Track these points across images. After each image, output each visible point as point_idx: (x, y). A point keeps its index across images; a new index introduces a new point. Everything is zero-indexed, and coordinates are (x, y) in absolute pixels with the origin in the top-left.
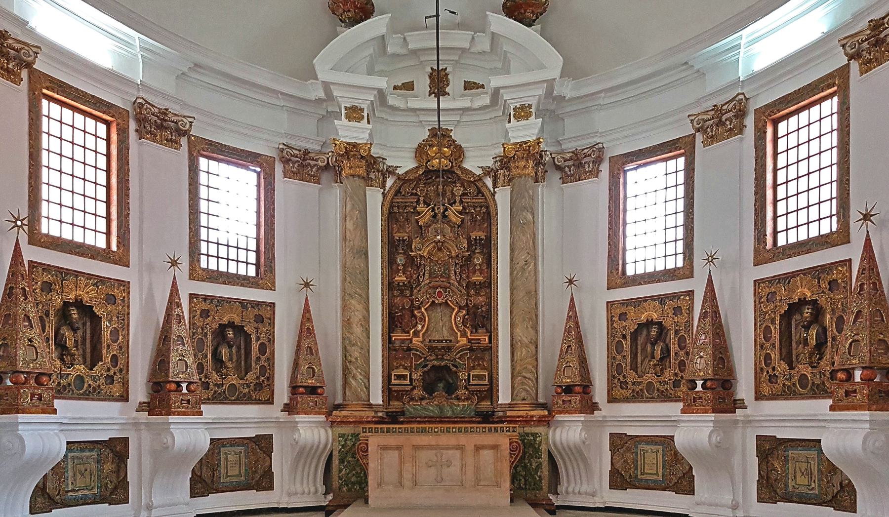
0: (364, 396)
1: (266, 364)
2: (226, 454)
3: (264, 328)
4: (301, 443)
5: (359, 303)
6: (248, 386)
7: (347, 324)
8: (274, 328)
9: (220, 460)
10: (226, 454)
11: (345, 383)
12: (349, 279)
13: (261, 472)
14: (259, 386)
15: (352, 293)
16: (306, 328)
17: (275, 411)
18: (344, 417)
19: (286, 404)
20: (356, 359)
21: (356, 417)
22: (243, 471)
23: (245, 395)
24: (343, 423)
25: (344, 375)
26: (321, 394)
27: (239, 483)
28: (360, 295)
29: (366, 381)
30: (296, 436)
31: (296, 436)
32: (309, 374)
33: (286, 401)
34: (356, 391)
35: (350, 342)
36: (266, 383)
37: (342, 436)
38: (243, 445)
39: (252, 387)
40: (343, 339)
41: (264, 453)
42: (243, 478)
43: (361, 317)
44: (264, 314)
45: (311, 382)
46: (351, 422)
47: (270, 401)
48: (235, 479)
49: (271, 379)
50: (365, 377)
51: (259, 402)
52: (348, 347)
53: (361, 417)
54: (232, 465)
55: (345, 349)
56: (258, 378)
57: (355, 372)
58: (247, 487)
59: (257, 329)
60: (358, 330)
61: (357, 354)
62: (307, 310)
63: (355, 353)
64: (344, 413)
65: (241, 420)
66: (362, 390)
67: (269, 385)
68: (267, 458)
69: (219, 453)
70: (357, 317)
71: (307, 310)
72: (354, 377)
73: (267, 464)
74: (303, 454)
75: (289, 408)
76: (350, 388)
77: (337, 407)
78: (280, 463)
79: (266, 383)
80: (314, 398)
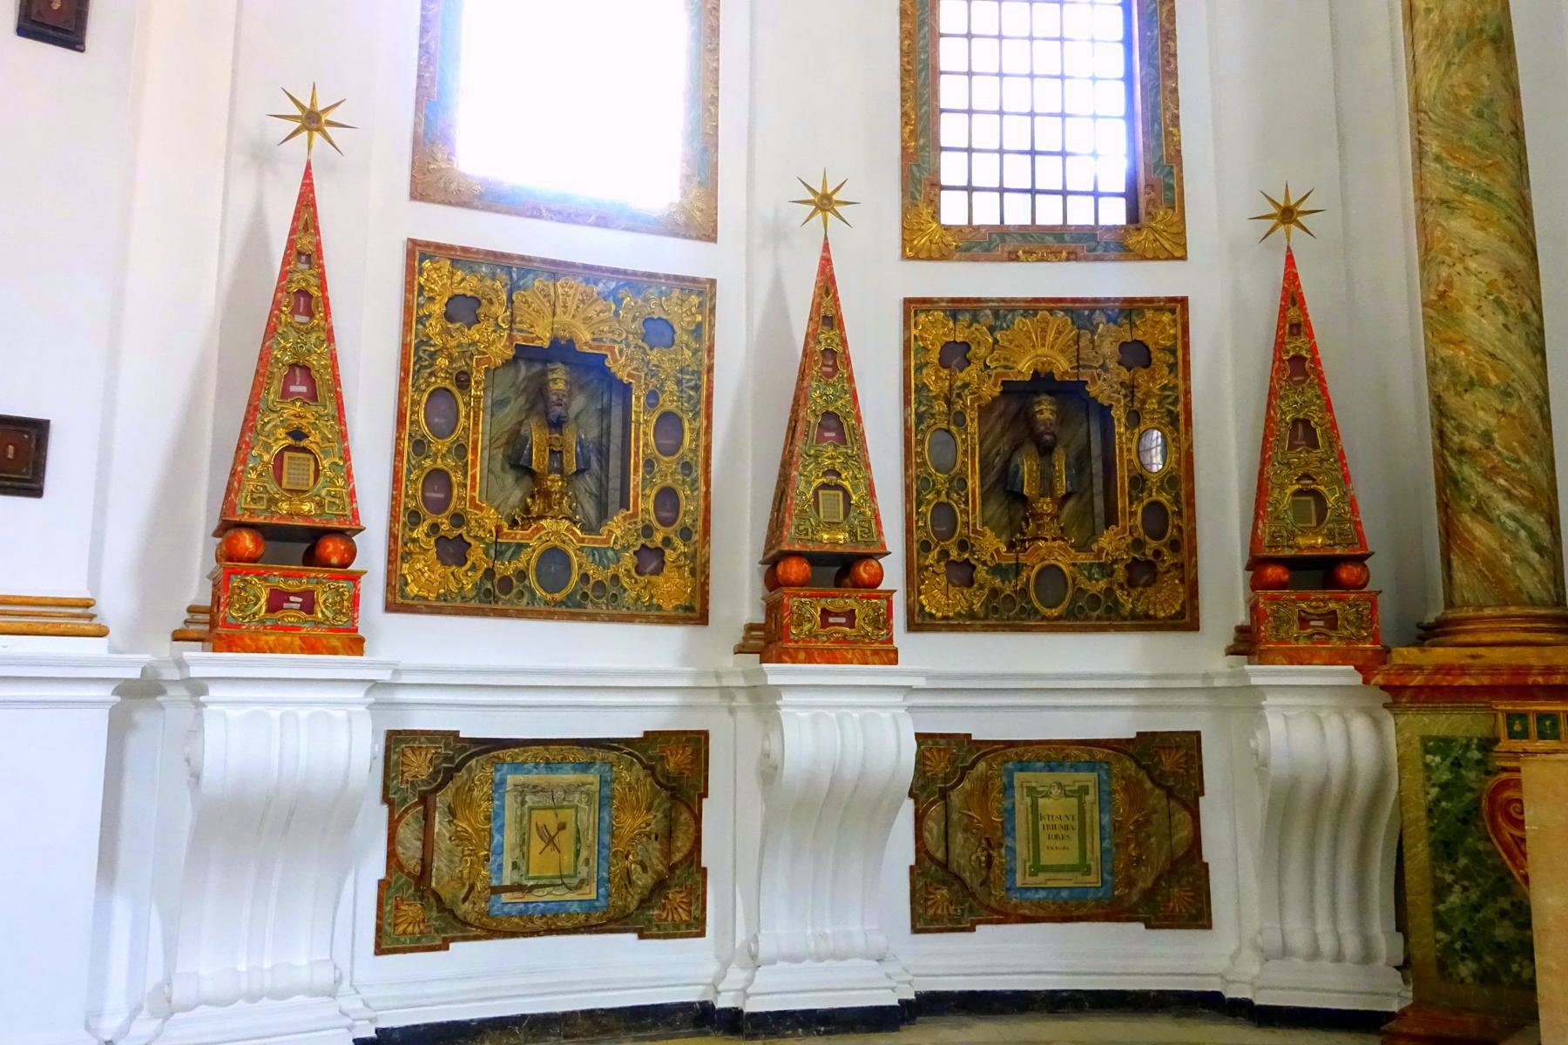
0: (1530, 581)
1: (1164, 498)
2: (1031, 791)
3: (1152, 383)
4: (1279, 765)
5: (1483, 223)
6: (1107, 570)
7: (1440, 308)
8: (1187, 377)
9: (1011, 812)
10: (1031, 791)
11: (1450, 534)
12: (1433, 147)
13: (1160, 860)
14: (1142, 572)
15: (1450, 193)
16: (1295, 361)
17: (1203, 654)
18: (1439, 669)
19: (1241, 630)
20: (1487, 437)
21: (1494, 669)
22: (1095, 845)
23: (1095, 599)
24: (1439, 692)
25: (1444, 506)
26: (1358, 586)
27: (1079, 893)
28: (1488, 195)
29: (1536, 522)
30: (1258, 742)
31: (1258, 742)
32: (1300, 515)
33: (1242, 618)
34: (1491, 563)
35: (1455, 374)
36: (1168, 558)
37: (1442, 745)
38: (1091, 766)
39: (1120, 573)
40: (1432, 370)
41: (1170, 794)
42: (1092, 880)
43: (1495, 274)
44: (1151, 341)
45: (1313, 542)
46: (1468, 689)
47: (1186, 620)
48: (1065, 881)
49: (1184, 546)
50: (1531, 506)
51: (1144, 622)
52: (1450, 399)
53: (1521, 670)
54: (1055, 831)
55: (1439, 407)
56: (1138, 544)
57: (1483, 488)
58: (1111, 911)
59: (1131, 388)
60: (1483, 326)
61: (1485, 419)
62: (1292, 296)
63: (1479, 412)
64: (1441, 654)
65: (1072, 683)
66: (1521, 560)
67: (1180, 566)
68: (1182, 816)
69: (1008, 788)
70: (1474, 281)
71: (1292, 296)
72: (1482, 511)
73: (1185, 833)
74: (1296, 809)
75: (1247, 644)
76: (1469, 554)
77: (1429, 634)
78: (1228, 833)
79: (1168, 558)
80: (1320, 600)
